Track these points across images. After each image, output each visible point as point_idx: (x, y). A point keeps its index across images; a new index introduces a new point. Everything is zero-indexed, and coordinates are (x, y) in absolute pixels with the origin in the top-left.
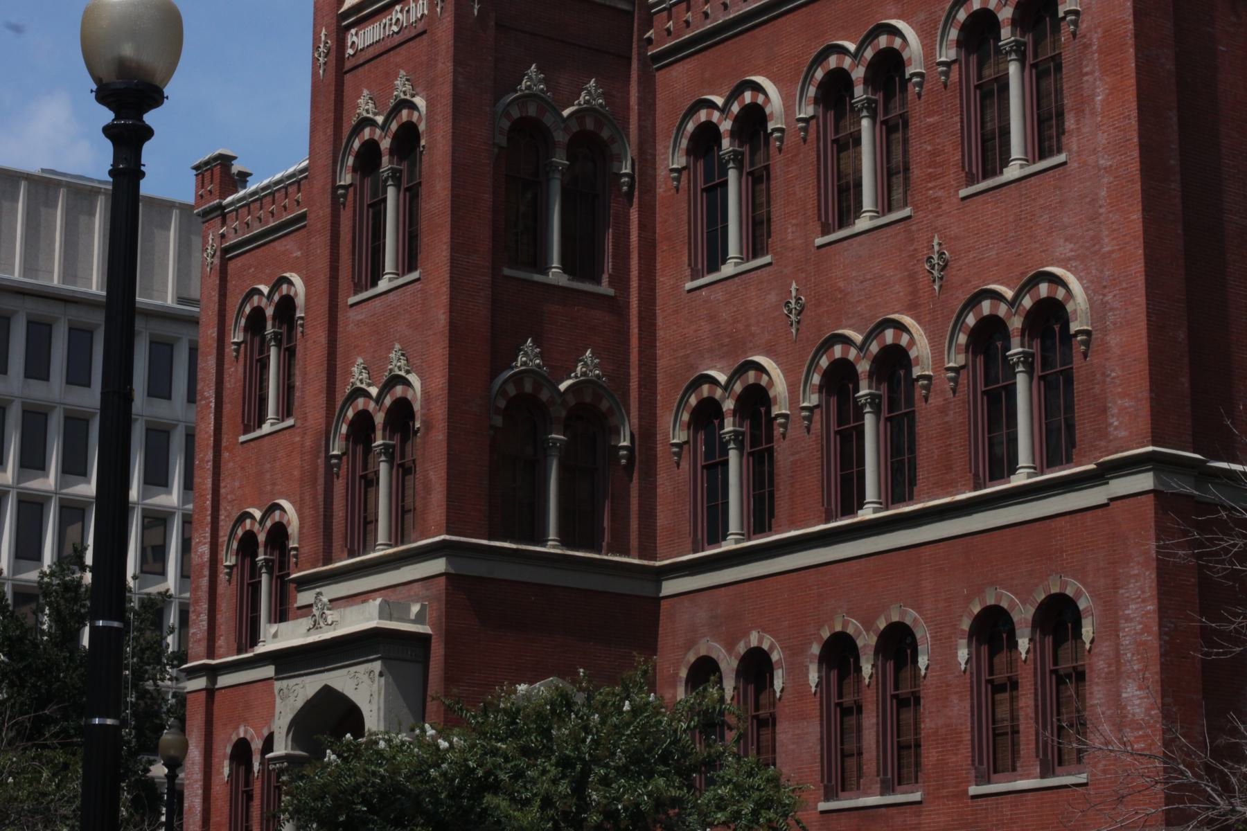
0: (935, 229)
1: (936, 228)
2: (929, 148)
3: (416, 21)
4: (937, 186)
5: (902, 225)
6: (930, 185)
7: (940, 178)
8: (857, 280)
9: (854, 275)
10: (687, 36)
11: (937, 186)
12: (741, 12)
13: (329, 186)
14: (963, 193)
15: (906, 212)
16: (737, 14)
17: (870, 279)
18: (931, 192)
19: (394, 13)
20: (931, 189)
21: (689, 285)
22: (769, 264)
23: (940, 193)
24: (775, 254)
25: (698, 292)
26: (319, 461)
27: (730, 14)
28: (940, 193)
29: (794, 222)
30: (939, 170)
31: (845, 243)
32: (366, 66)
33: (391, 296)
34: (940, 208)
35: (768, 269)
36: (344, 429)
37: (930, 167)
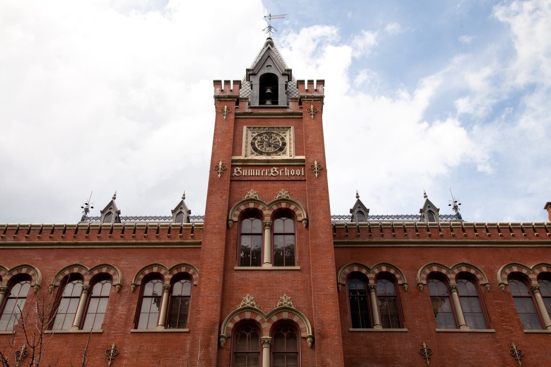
0: (512, 341)
1: (512, 340)
2: (499, 311)
3: (289, 176)
4: (508, 325)
5: (490, 335)
6: (503, 324)
7: (509, 323)
8: (466, 350)
9: (463, 347)
10: (346, 240)
11: (508, 325)
12: (380, 240)
13: (225, 218)
14: (525, 331)
15: (493, 330)
16: (377, 240)
17: (474, 351)
18: (505, 326)
19: (272, 169)
20: (504, 325)
21: (351, 329)
22: (406, 332)
23: (511, 328)
24: (409, 329)
25: (357, 334)
26: (212, 336)
27: (373, 239)
28: (511, 328)
29: (419, 319)
30: (508, 320)
31: (455, 334)
32: (248, 182)
33: (274, 273)
34: (513, 333)
35: (405, 334)
36: (231, 325)
37: (502, 317)
